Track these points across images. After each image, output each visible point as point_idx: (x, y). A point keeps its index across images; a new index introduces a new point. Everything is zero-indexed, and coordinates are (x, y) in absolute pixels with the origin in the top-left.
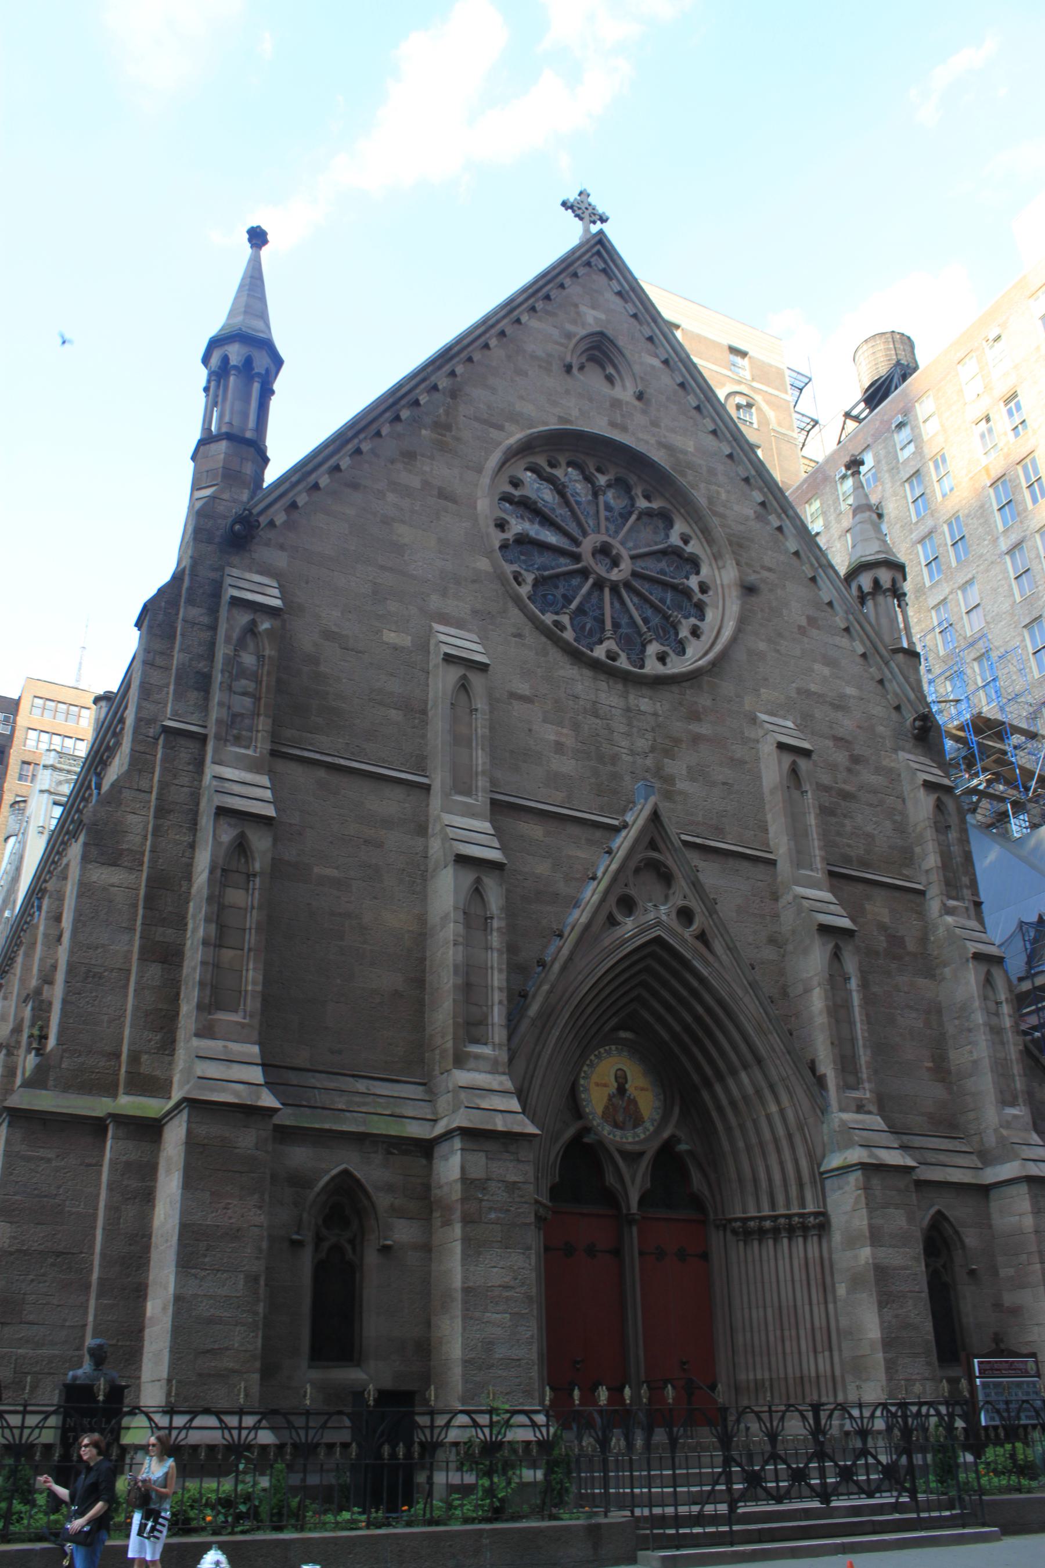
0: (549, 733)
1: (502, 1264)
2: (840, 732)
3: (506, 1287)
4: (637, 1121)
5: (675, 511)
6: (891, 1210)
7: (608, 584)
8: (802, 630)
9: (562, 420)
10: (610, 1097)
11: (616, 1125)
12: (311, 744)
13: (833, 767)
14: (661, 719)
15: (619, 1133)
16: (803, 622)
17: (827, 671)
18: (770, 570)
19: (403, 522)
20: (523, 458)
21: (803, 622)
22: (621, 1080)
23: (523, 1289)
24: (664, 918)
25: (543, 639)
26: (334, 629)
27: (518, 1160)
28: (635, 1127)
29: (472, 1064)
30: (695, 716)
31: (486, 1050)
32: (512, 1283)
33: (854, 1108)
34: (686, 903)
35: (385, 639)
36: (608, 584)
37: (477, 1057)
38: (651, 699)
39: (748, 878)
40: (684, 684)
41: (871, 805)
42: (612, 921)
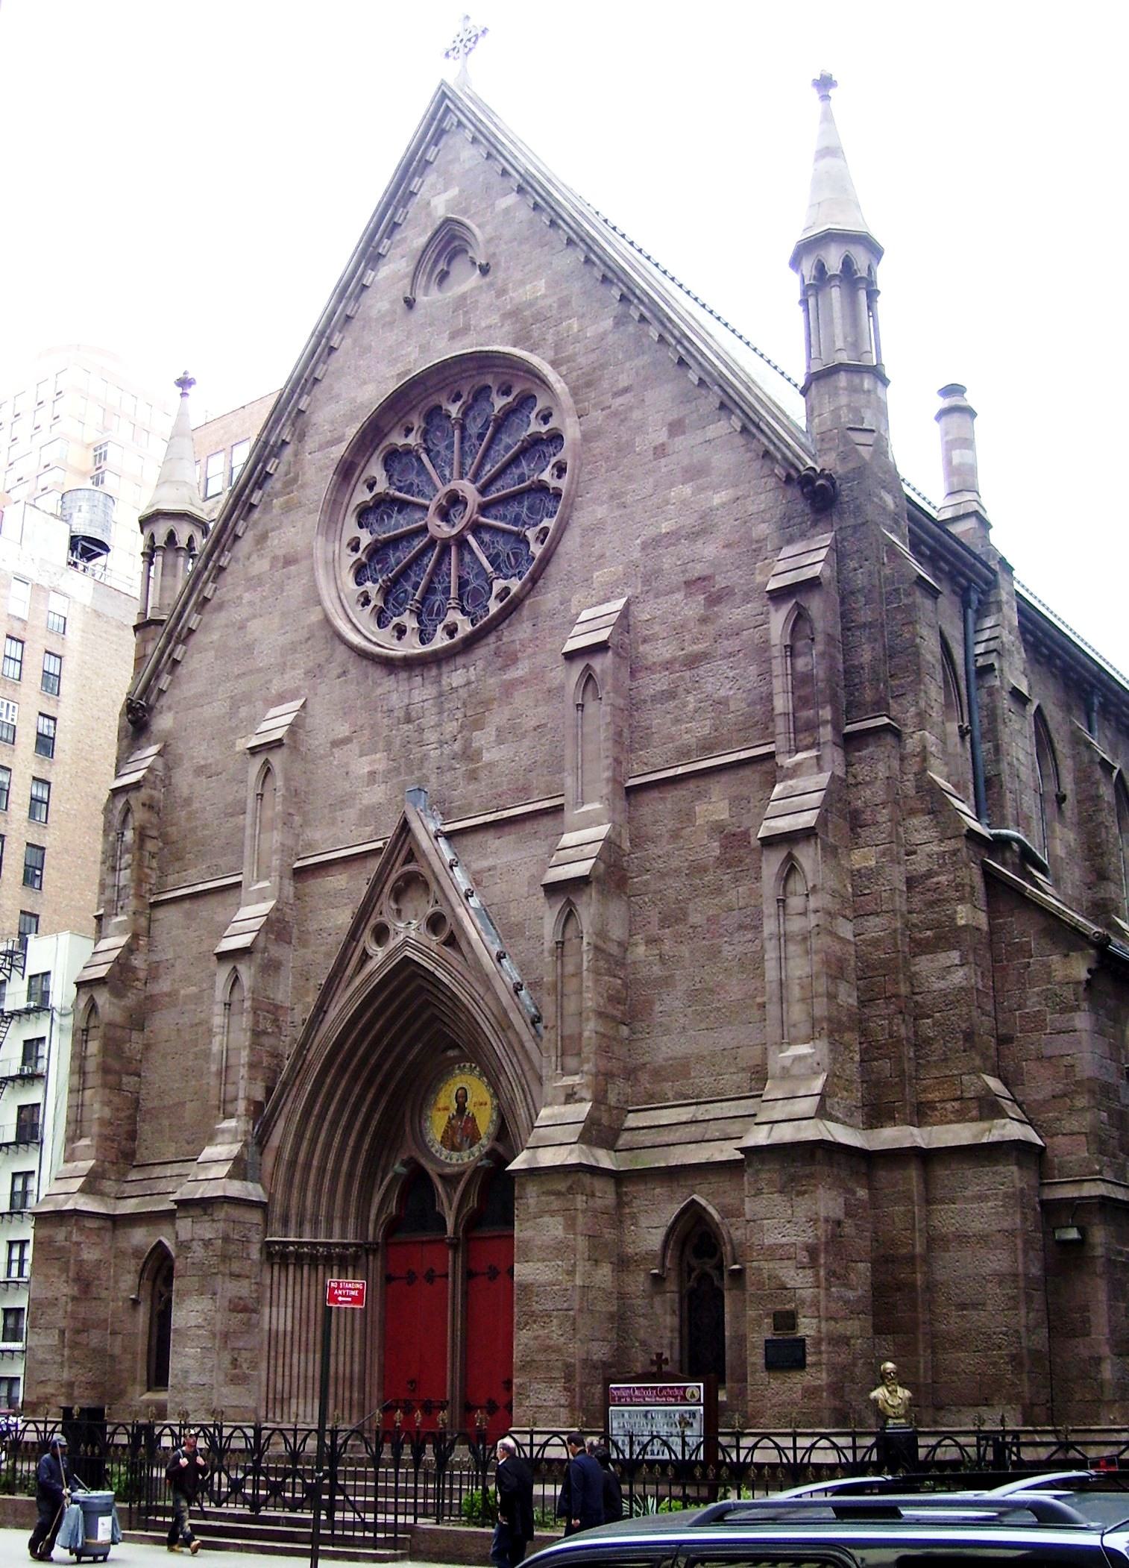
0: (362, 766)
1: (199, 1308)
2: (698, 570)
3: (198, 1327)
4: (474, 1137)
5: (535, 387)
6: (546, 1219)
7: (452, 542)
8: (660, 451)
9: (400, 376)
10: (450, 1119)
11: (454, 1148)
12: (185, 881)
13: (679, 631)
14: (473, 686)
15: (455, 1155)
16: (662, 436)
17: (687, 490)
18: (626, 390)
19: (254, 617)
20: (375, 449)
21: (662, 436)
22: (462, 1097)
23: (209, 1328)
24: (413, 934)
25: (365, 662)
26: (202, 763)
27: (213, 1221)
28: (471, 1146)
29: (219, 1139)
30: (512, 660)
31: (231, 1124)
32: (203, 1324)
33: (563, 1099)
34: (437, 908)
35: (237, 749)
36: (452, 542)
37: (223, 1131)
38: (464, 666)
39: (547, 837)
40: (501, 627)
41: (731, 655)
42: (366, 957)
